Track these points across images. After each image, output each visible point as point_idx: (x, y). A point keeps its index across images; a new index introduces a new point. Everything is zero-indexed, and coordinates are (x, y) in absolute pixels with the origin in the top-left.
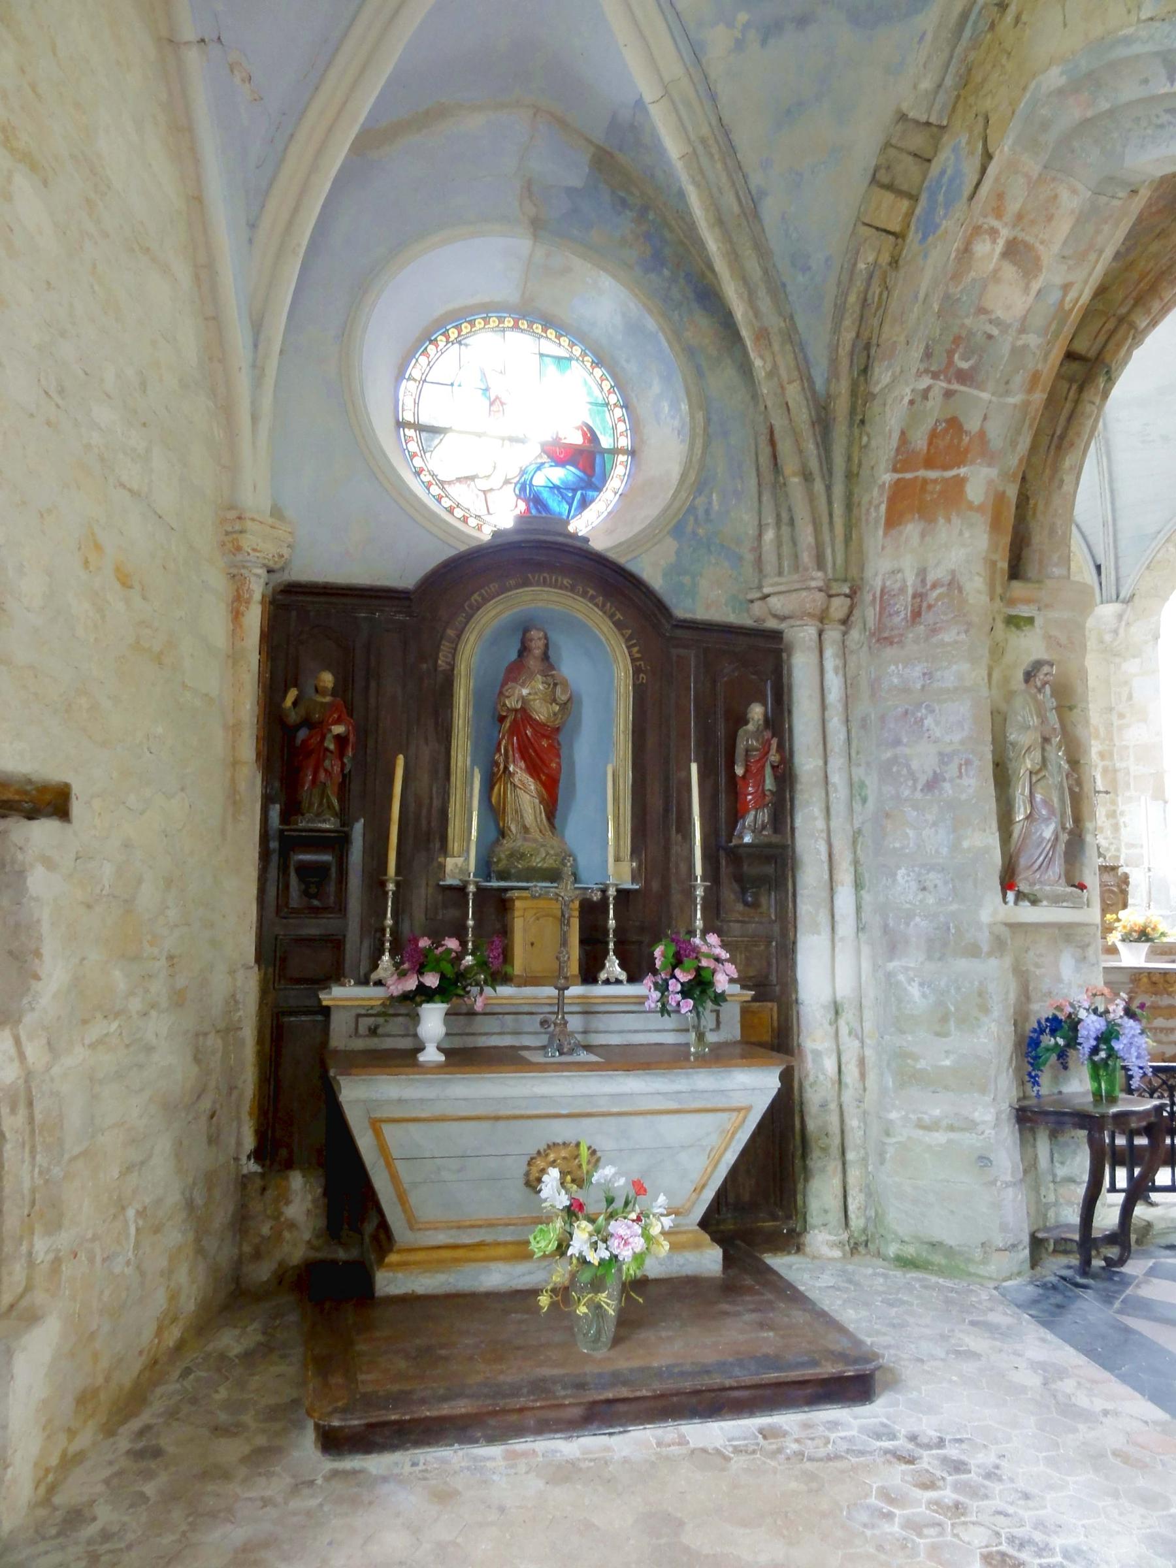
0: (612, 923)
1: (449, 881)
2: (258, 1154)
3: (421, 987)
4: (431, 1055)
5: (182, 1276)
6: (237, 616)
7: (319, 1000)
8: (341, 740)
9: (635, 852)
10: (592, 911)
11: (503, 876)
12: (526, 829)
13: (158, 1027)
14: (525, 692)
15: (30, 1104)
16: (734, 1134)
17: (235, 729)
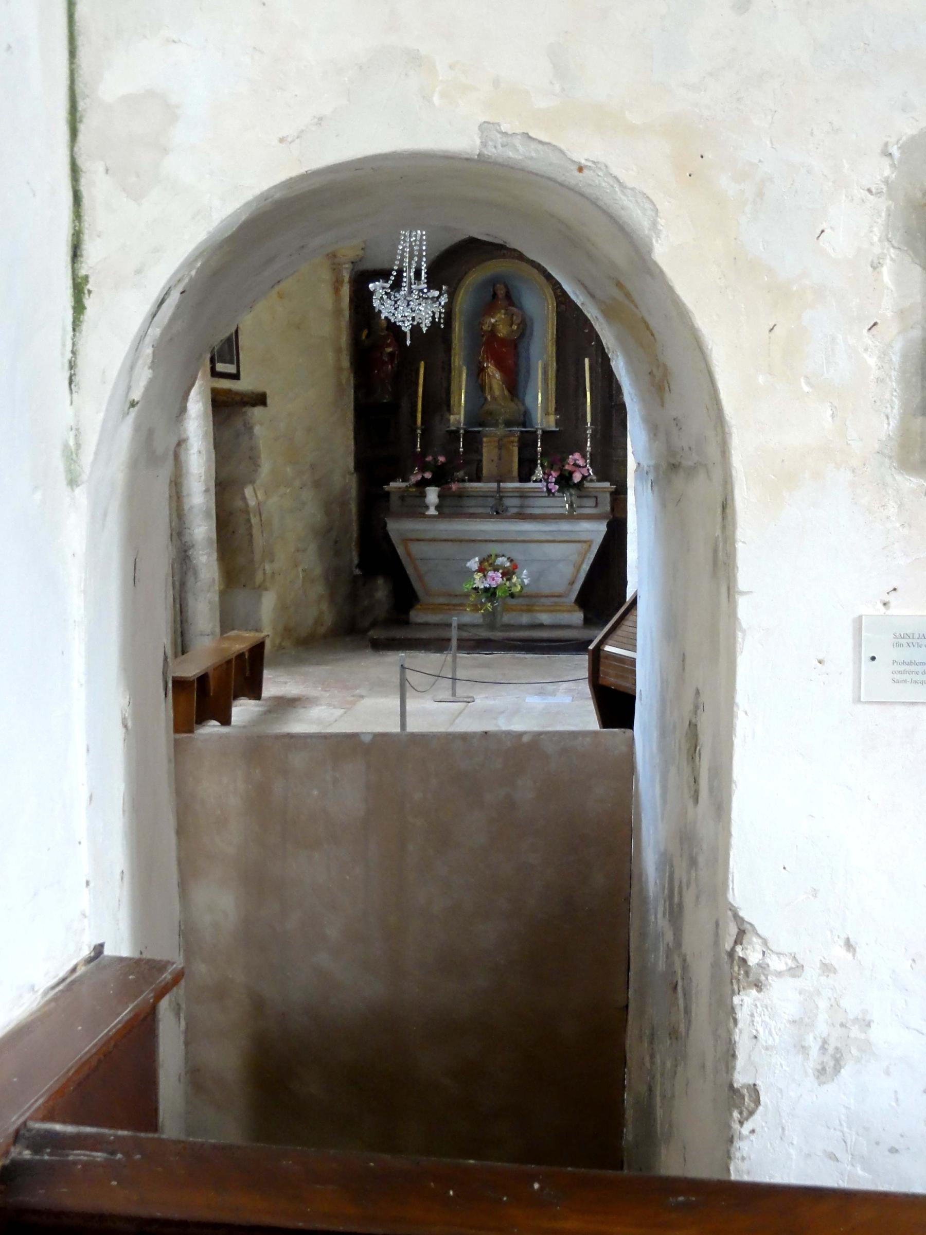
0: (539, 449)
1: (453, 428)
2: (359, 566)
3: (423, 478)
4: (432, 511)
5: (324, 606)
6: (337, 290)
7: (383, 489)
8: (391, 355)
9: (557, 410)
10: (527, 442)
11: (481, 425)
12: (494, 398)
13: (308, 495)
14: (493, 321)
15: (260, 515)
16: (585, 554)
17: (338, 350)
